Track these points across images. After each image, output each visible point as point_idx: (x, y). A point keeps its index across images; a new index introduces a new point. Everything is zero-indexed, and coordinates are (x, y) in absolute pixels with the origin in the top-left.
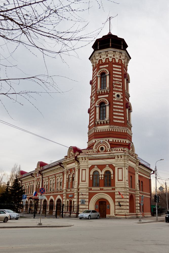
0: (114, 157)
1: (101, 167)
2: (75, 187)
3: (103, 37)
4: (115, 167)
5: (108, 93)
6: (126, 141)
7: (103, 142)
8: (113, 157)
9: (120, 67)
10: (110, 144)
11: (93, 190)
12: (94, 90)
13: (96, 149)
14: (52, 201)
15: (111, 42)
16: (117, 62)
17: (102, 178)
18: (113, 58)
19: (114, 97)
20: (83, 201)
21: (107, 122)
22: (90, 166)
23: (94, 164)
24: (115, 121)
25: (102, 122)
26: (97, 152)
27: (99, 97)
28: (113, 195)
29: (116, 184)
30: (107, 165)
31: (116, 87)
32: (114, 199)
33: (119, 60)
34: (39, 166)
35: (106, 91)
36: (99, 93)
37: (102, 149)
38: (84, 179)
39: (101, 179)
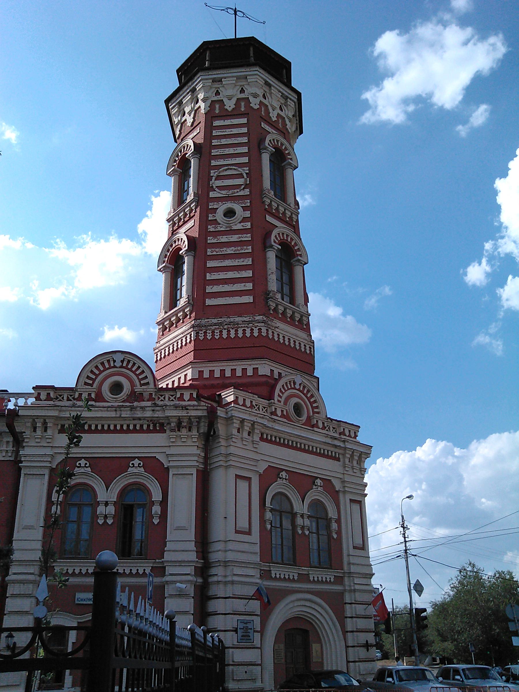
4: (338, 492)
20: (247, 628)
22: (262, 467)
23: (278, 463)
25: (289, 313)
28: (337, 603)
32: (342, 618)
36: (270, 205)
37: (297, 409)
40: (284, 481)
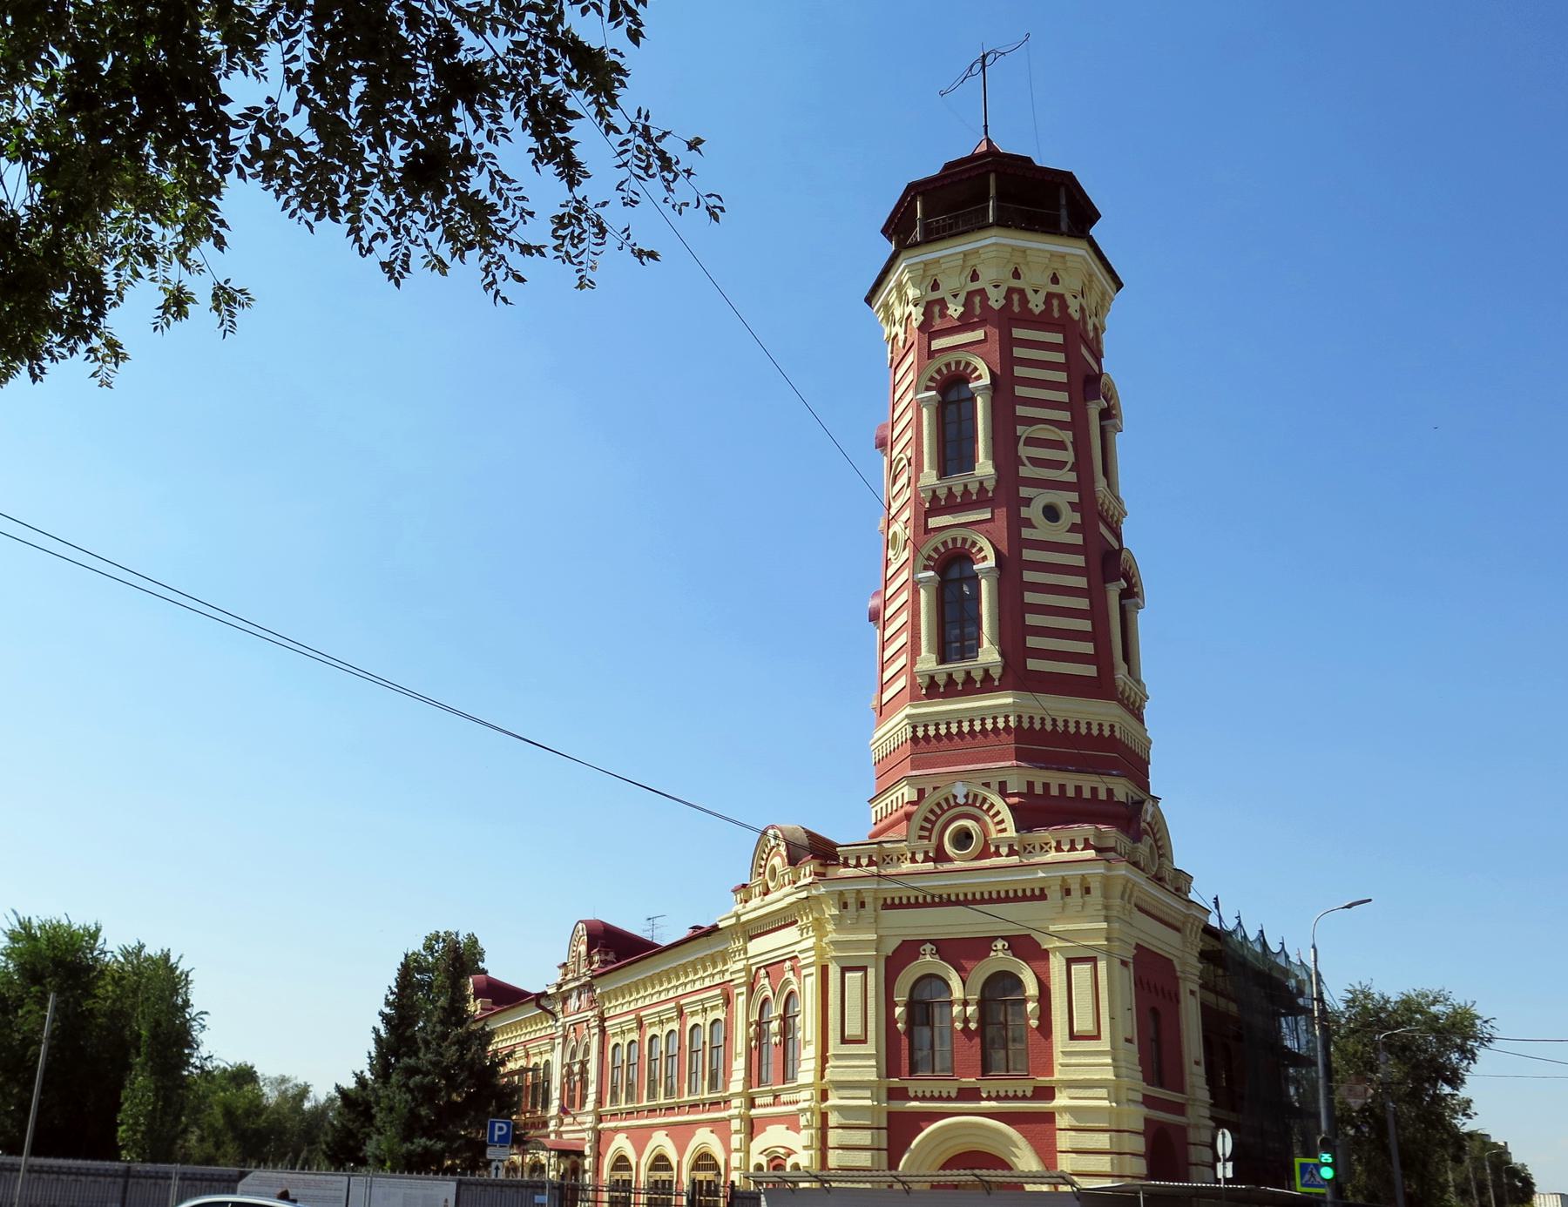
0: (1042, 890)
1: (962, 952)
2: (806, 1071)
3: (948, 166)
5: (992, 499)
6: (1110, 792)
7: (966, 796)
8: (1037, 892)
9: (1058, 338)
10: (1012, 807)
11: (912, 1094)
12: (903, 480)
13: (929, 838)
14: (660, 1163)
15: (992, 192)
16: (1037, 311)
17: (966, 1021)
18: (1010, 291)
19: (1028, 523)
21: (986, 671)
22: (891, 946)
24: (1033, 664)
26: (935, 861)
27: (933, 522)
29: (1058, 1059)
30: (996, 938)
31: (1036, 462)
33: (1050, 296)
34: (583, 948)
35: (974, 488)
38: (853, 1029)
39: (966, 1030)
40: (928, 958)
